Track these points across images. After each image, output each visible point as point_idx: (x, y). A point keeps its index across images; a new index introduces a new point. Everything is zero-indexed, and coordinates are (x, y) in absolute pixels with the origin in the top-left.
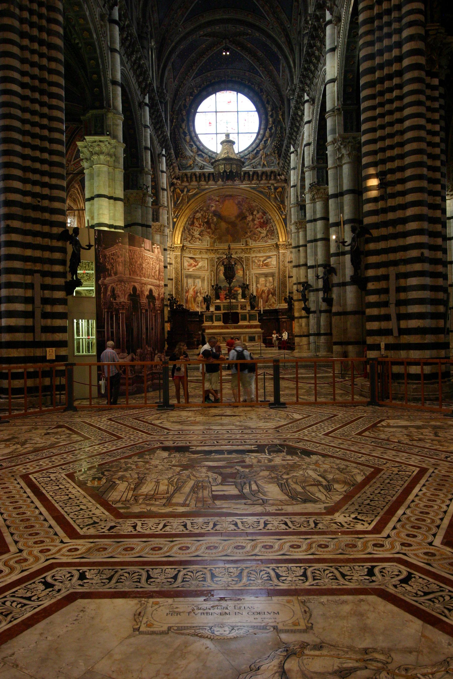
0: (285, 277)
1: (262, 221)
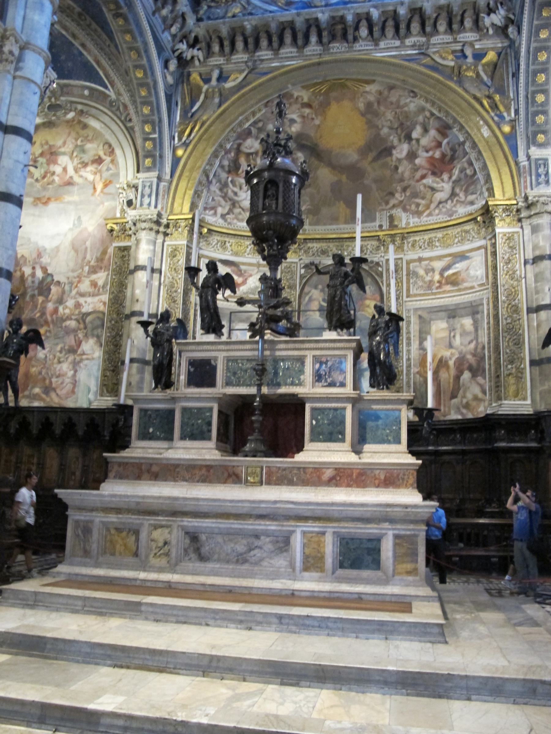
0: (516, 309)
1: (437, 155)
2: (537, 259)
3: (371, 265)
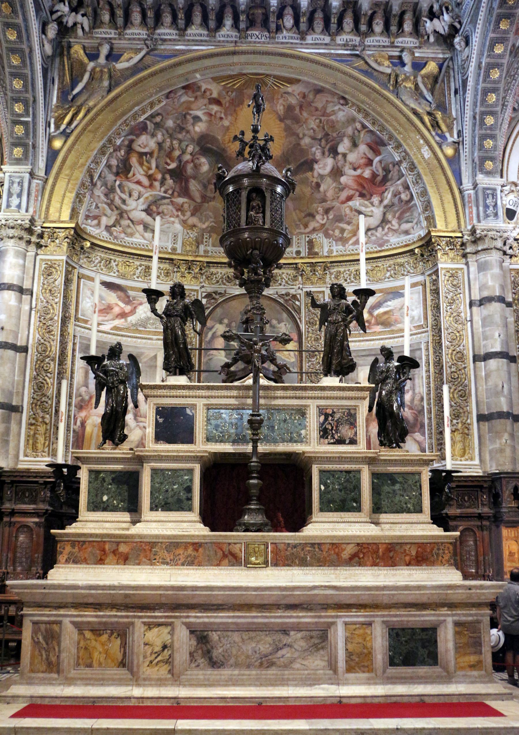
0: (461, 357)
1: (367, 174)
2: (483, 302)
3: (287, 298)
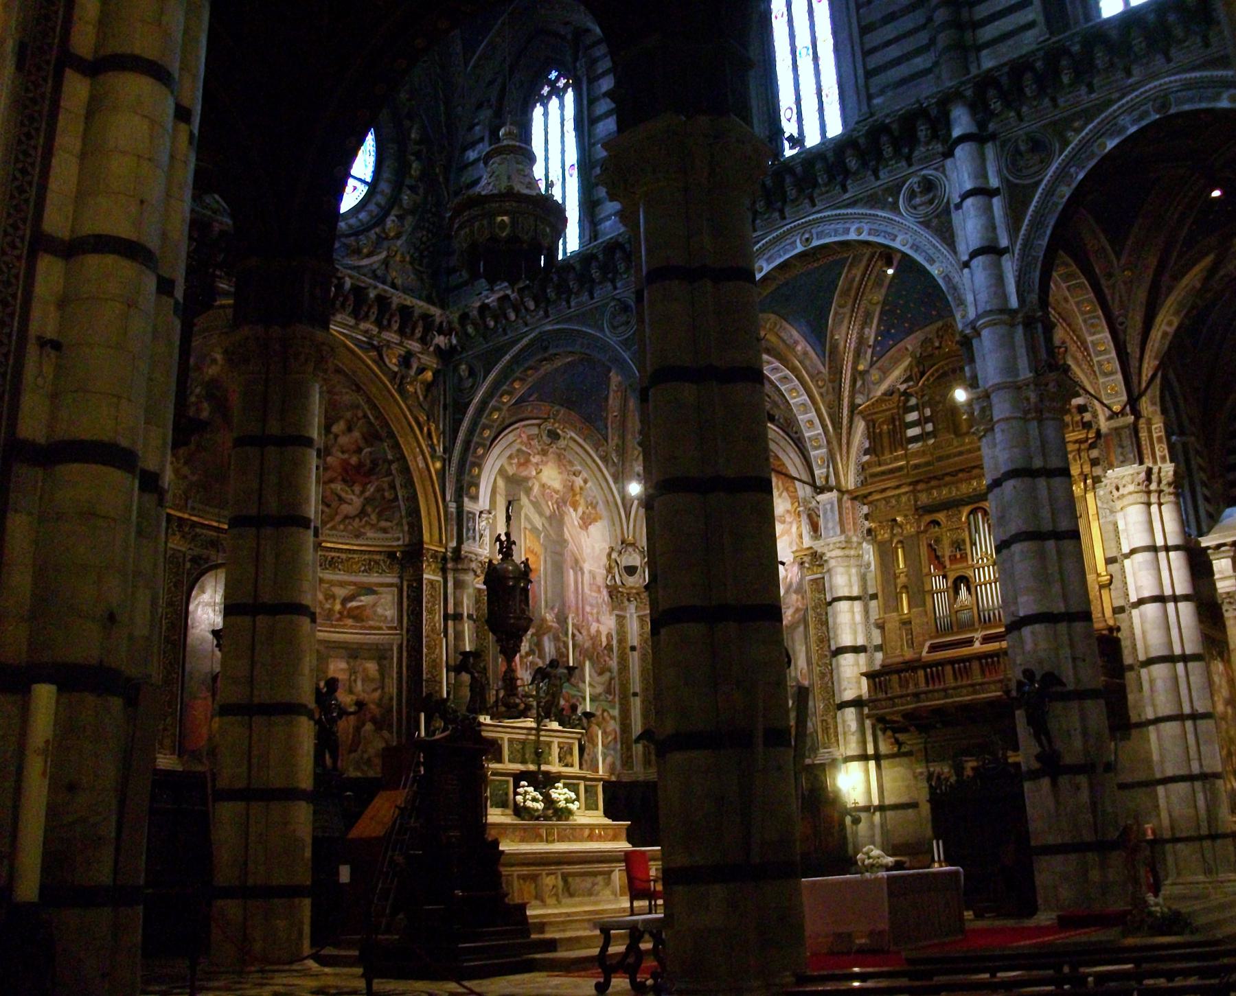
1: (354, 460)
